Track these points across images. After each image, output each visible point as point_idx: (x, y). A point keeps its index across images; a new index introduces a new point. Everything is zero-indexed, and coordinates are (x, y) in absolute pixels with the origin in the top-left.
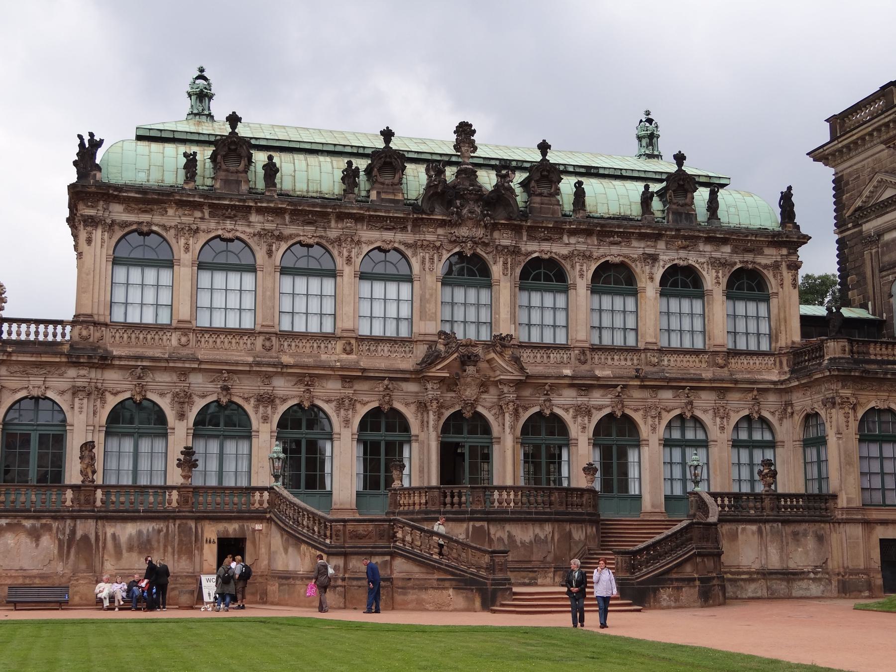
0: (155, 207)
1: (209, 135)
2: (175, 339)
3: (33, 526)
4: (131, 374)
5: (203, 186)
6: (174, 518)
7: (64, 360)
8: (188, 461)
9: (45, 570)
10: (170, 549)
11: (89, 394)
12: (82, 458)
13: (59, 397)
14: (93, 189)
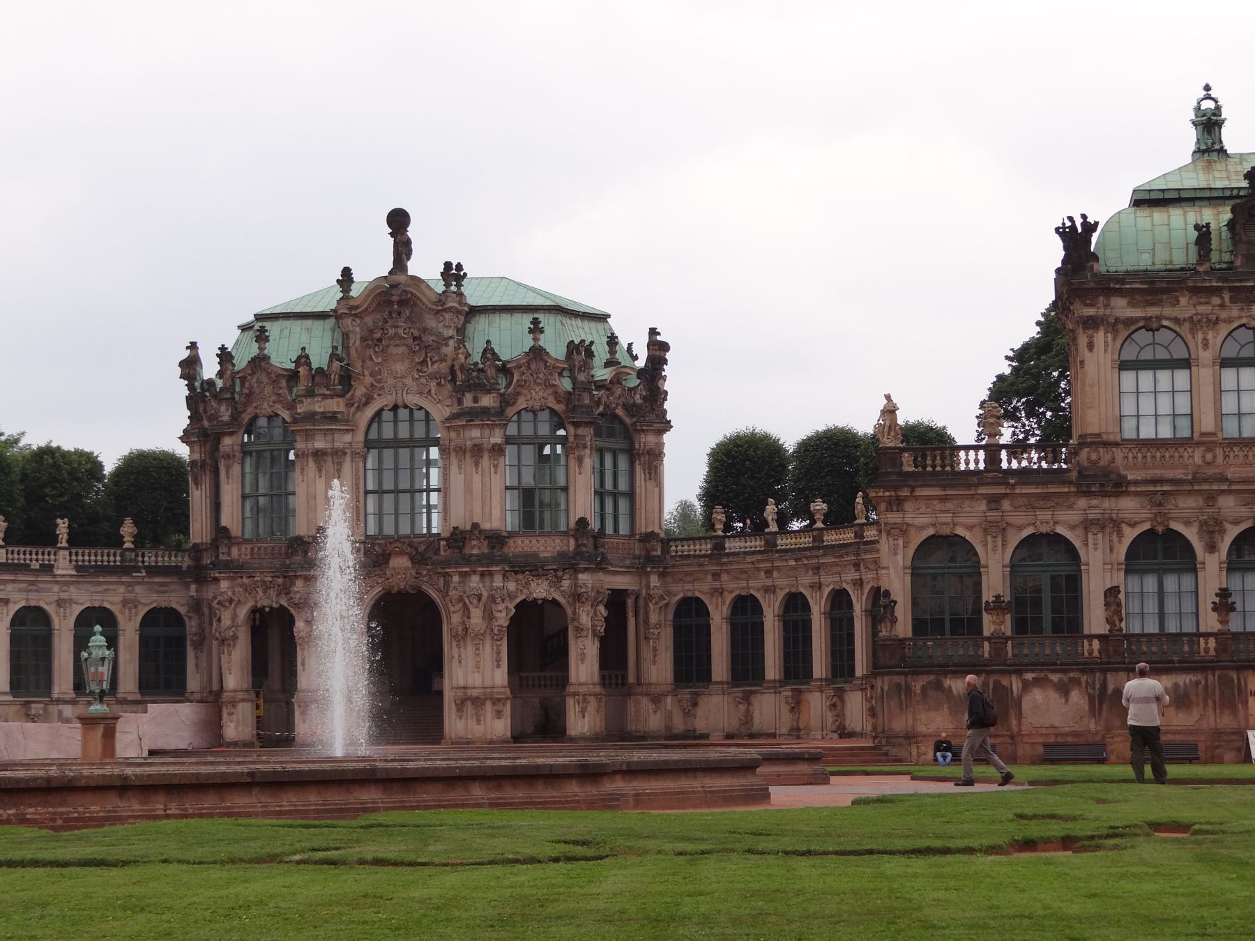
0: (1164, 297)
1: (1223, 189)
2: (1197, 455)
3: (1061, 680)
4: (1150, 501)
5: (1220, 263)
6: (1213, 669)
7: (1073, 489)
8: (1224, 603)
9: (1076, 728)
10: (1210, 703)
11: (1103, 528)
12: (1107, 605)
13: (1070, 533)
14: (1092, 285)
